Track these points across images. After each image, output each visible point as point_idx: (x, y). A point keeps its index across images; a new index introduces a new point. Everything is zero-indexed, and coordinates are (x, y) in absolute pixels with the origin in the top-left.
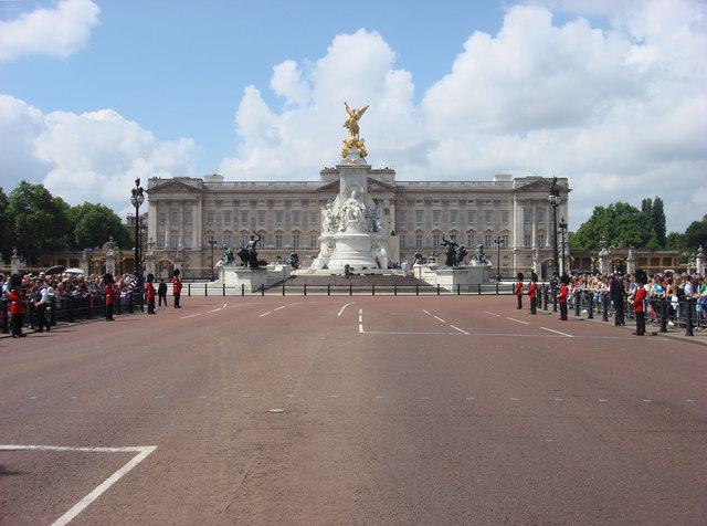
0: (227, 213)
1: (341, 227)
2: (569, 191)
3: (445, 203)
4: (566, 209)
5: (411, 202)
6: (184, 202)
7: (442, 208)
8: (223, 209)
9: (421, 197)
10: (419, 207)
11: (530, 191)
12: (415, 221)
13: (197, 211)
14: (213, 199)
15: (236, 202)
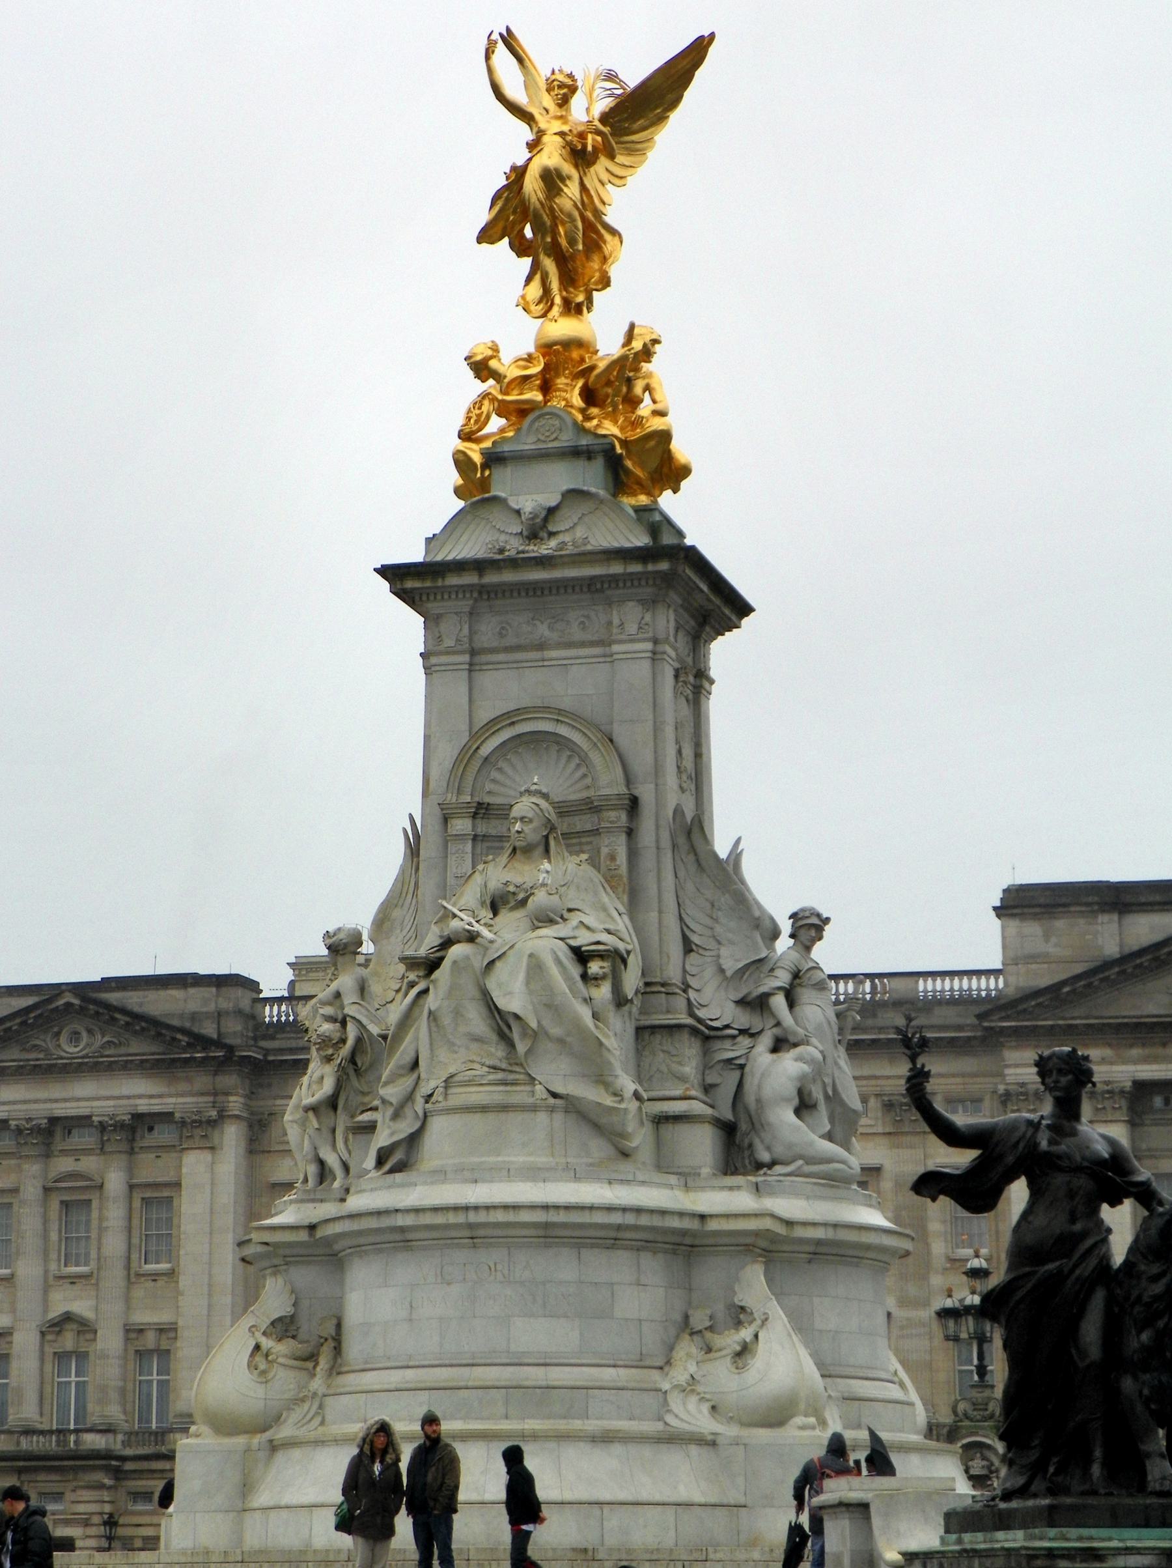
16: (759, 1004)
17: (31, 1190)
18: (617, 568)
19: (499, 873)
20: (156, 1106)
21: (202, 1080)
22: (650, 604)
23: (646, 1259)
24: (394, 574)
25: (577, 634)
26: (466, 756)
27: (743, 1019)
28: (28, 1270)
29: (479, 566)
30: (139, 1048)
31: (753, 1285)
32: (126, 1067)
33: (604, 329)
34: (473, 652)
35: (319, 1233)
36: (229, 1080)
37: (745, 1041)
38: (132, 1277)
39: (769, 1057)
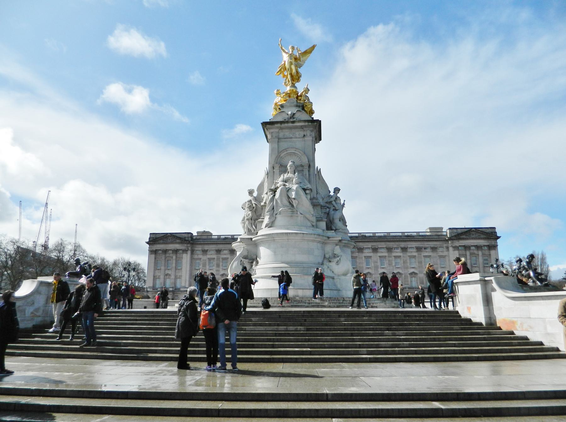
0: (210, 259)
1: (266, 220)
2: (499, 237)
3: (389, 250)
4: (497, 254)
5: (361, 250)
6: (176, 251)
7: (386, 254)
8: (209, 256)
9: (370, 245)
10: (367, 253)
11: (463, 239)
12: (364, 265)
13: (186, 258)
14: (200, 249)
15: (218, 251)
16: (331, 202)
17: (163, 258)
18: (307, 124)
19: (286, 176)
20: (180, 248)
21: (186, 245)
22: (312, 131)
23: (319, 244)
24: (265, 125)
25: (298, 136)
26: (278, 157)
27: (327, 205)
28: (163, 268)
29: (281, 122)
30: (178, 241)
31: (338, 250)
32: (176, 243)
33: (300, 87)
34: (279, 139)
35: (253, 239)
36: (189, 245)
37: (328, 209)
38: (176, 269)
39: (333, 212)
